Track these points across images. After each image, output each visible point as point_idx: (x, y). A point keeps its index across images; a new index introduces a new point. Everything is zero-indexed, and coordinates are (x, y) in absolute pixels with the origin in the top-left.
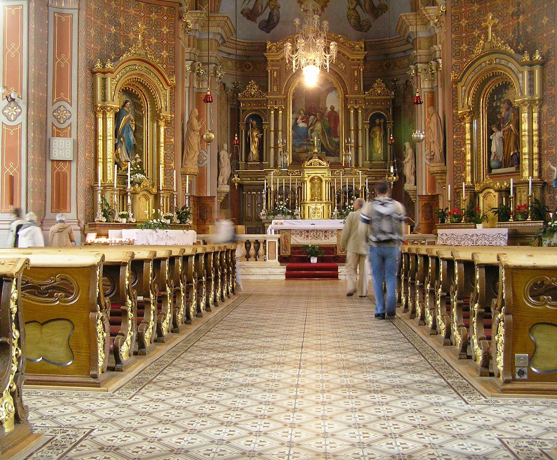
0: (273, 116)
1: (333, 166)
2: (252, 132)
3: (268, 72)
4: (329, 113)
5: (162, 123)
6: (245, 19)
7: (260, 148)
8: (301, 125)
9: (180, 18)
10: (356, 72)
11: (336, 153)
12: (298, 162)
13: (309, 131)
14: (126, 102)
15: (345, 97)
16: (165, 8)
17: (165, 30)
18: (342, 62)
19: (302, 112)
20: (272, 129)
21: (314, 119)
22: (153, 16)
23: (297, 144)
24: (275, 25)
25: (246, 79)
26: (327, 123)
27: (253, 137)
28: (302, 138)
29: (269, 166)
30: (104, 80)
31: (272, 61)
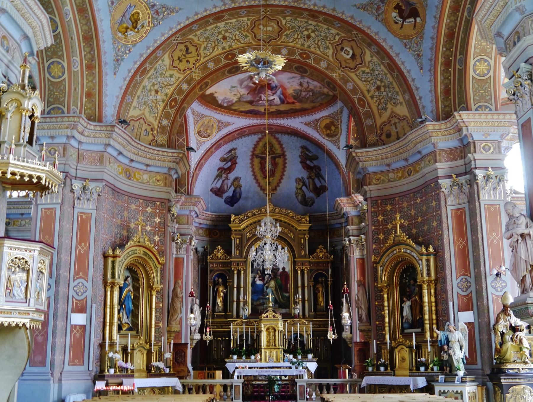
0: (236, 275)
1: (286, 316)
2: (218, 288)
3: (232, 240)
4: (281, 272)
5: (154, 293)
6: (214, 195)
7: (225, 302)
8: (259, 282)
9: (169, 210)
10: (302, 240)
11: (287, 306)
12: (256, 313)
13: (265, 287)
14: (128, 277)
15: (294, 260)
16: (158, 203)
17: (157, 220)
18: (291, 232)
19: (259, 272)
20: (235, 286)
21: (269, 277)
22: (149, 210)
23: (255, 298)
24: (238, 200)
25: (213, 245)
26: (279, 281)
27: (219, 292)
28: (259, 293)
29: (232, 317)
30: (113, 263)
31: (235, 231)
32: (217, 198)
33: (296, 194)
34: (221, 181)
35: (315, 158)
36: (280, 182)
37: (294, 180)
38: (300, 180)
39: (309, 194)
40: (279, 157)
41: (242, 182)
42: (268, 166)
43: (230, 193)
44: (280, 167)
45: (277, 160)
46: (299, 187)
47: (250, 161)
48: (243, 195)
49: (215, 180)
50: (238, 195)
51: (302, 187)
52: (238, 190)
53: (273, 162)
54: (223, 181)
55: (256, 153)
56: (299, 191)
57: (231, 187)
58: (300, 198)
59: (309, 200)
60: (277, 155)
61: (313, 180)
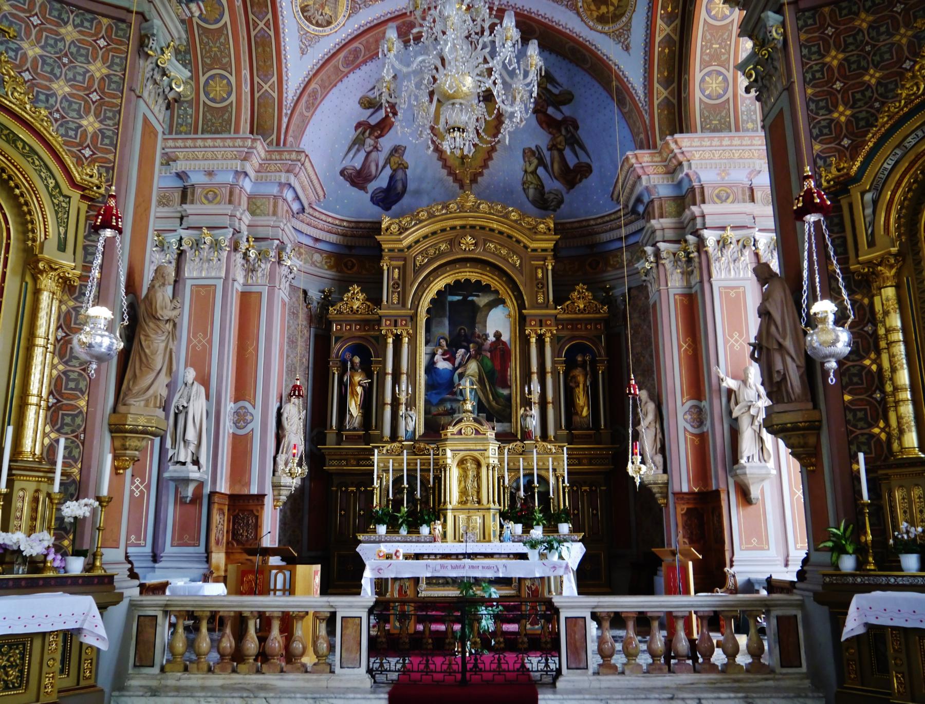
33: (524, 183)
34: (362, 155)
35: (567, 98)
37: (520, 153)
38: (533, 153)
41: (408, 158)
43: (382, 182)
46: (530, 169)
48: (411, 186)
49: (350, 149)
50: (400, 186)
51: (536, 168)
52: (400, 175)
54: (368, 154)
57: (384, 167)
58: (531, 191)
59: (552, 196)
61: (561, 152)
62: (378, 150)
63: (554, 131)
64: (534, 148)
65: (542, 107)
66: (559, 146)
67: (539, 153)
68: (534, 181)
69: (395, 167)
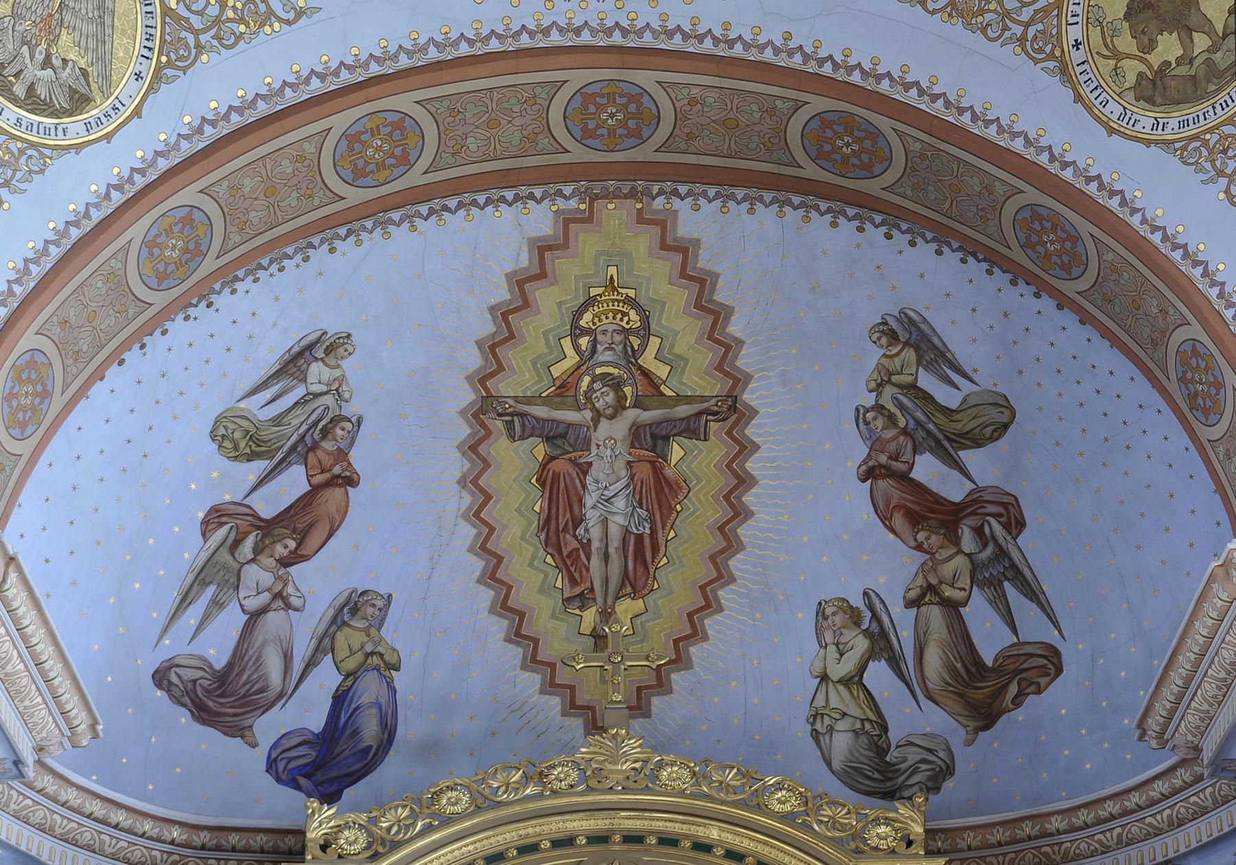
32: (210, 742)
33: (815, 716)
34: (231, 621)
36: (696, 633)
37: (807, 618)
38: (854, 616)
39: (914, 719)
40: (692, 429)
41: (397, 633)
42: (608, 507)
43: (308, 710)
44: (699, 513)
45: (676, 453)
46: (839, 670)
47: (457, 465)
48: (409, 729)
49: (185, 601)
50: (370, 730)
51: (862, 668)
52: (369, 690)
53: (644, 471)
54: (255, 616)
55: (506, 387)
56: (838, 698)
57: (311, 664)
59: (913, 755)
60: (683, 411)
62: (288, 606)
63: (934, 539)
64: (857, 601)
65: (896, 457)
66: (948, 592)
67: (875, 616)
68: (854, 710)
69: (352, 663)
